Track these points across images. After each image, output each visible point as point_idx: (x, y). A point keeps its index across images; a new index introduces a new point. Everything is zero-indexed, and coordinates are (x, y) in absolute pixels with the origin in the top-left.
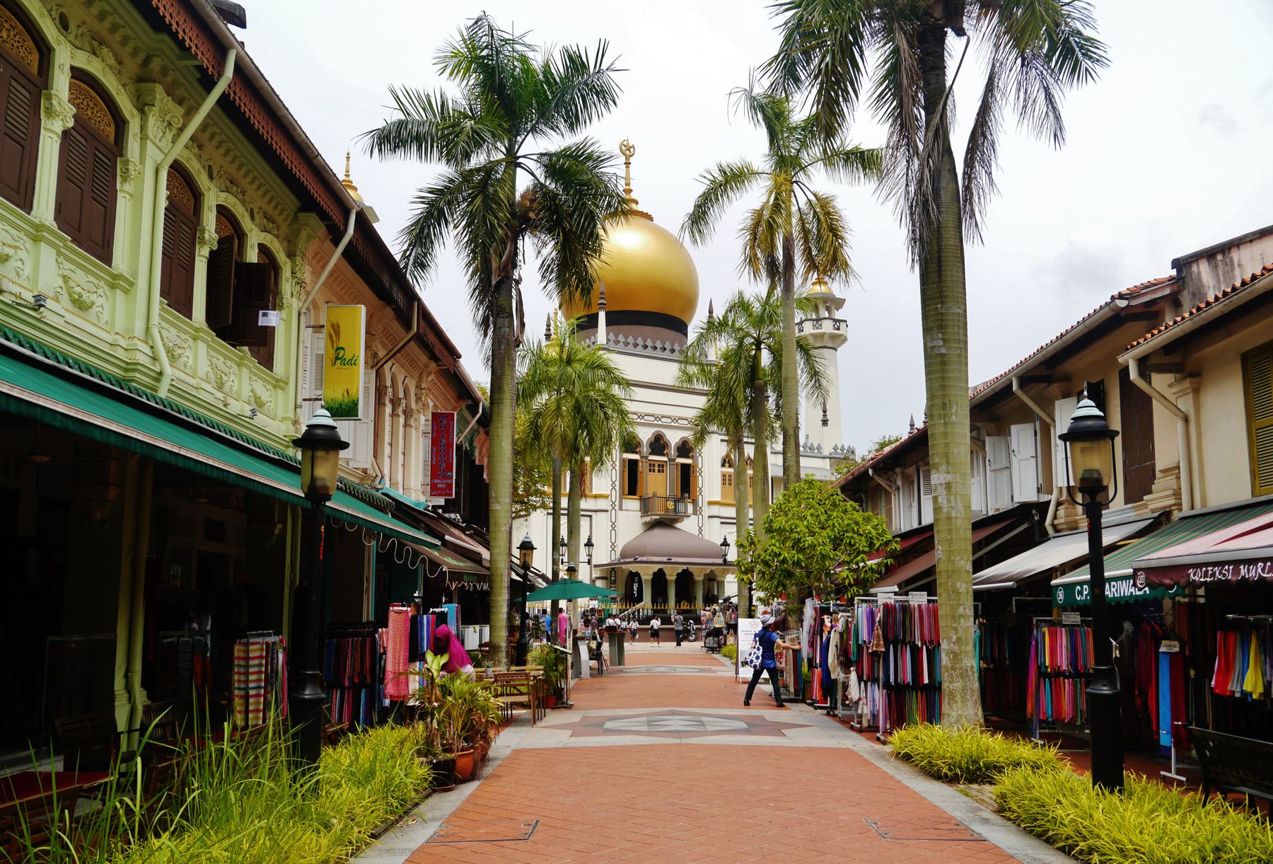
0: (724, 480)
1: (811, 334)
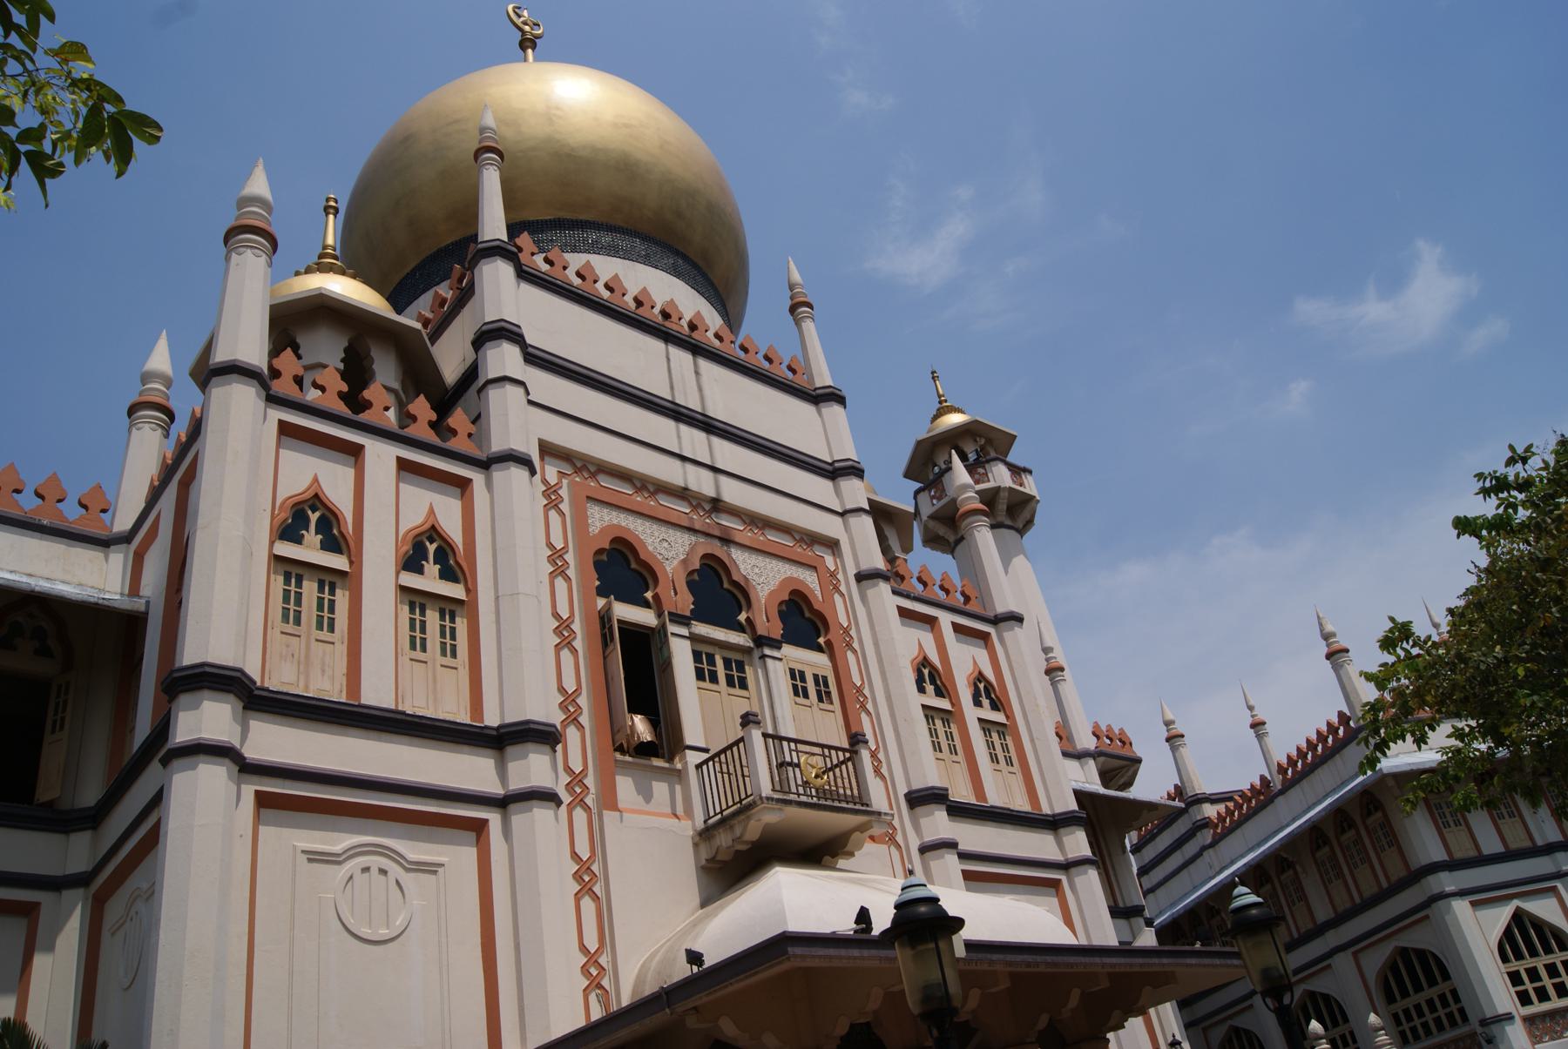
0: (933, 733)
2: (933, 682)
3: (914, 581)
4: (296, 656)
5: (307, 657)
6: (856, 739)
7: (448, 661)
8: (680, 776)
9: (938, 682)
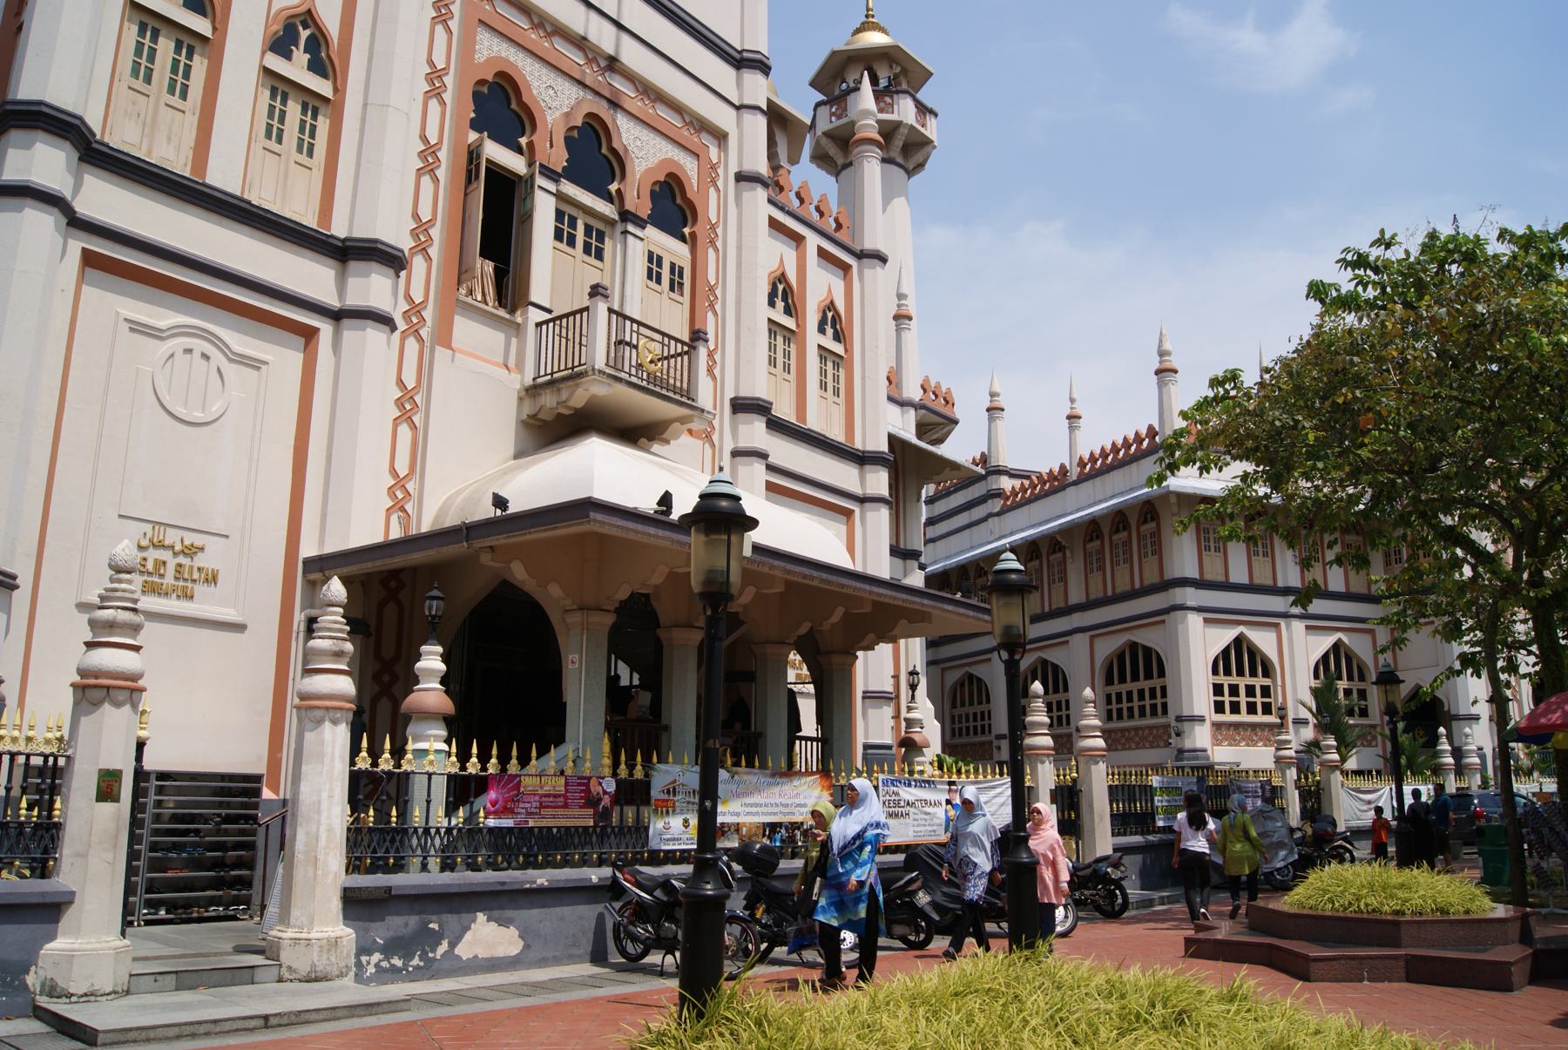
0: (772, 348)
2: (785, 299)
3: (792, 196)
4: (142, 116)
5: (154, 120)
6: (697, 336)
7: (303, 158)
8: (518, 329)
9: (790, 301)
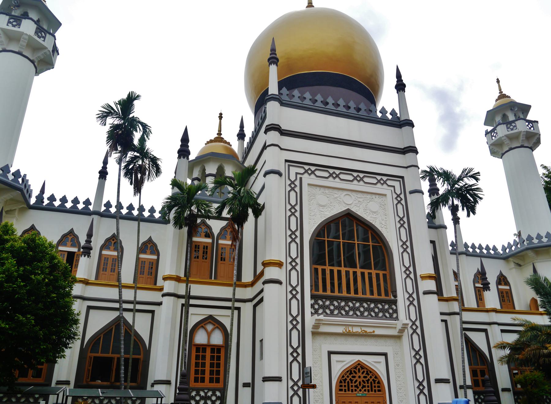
1: (506, 136)
